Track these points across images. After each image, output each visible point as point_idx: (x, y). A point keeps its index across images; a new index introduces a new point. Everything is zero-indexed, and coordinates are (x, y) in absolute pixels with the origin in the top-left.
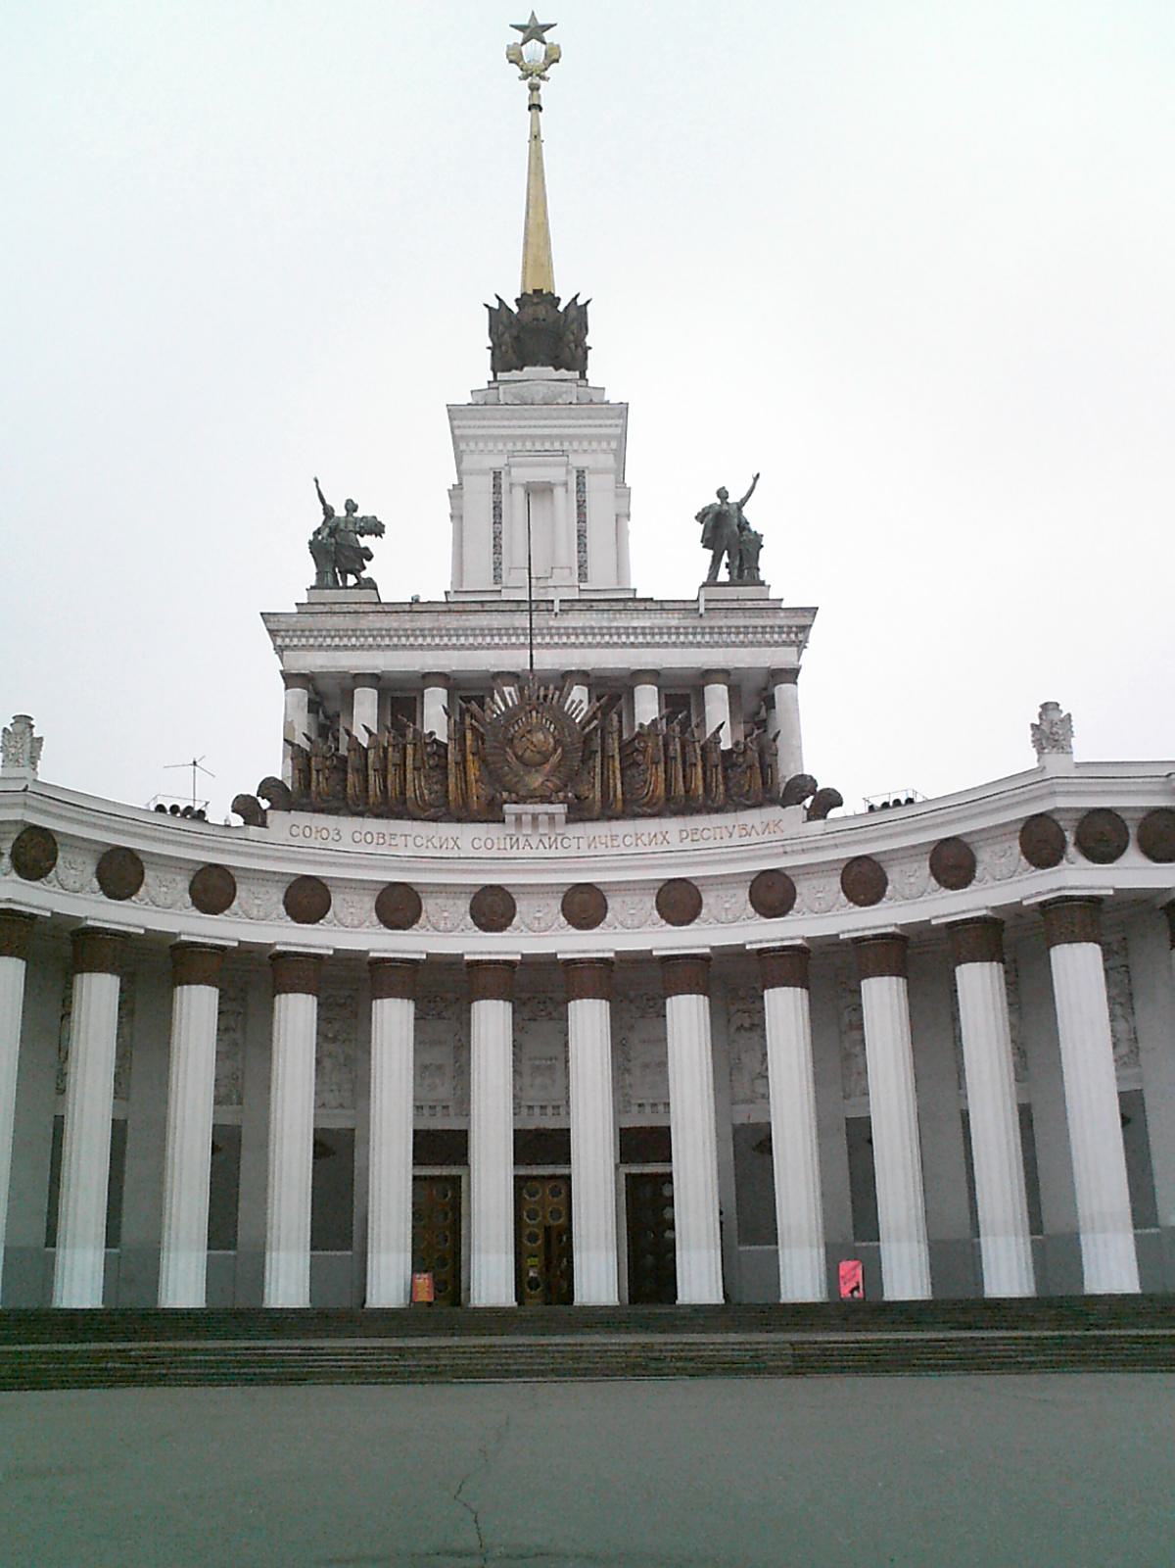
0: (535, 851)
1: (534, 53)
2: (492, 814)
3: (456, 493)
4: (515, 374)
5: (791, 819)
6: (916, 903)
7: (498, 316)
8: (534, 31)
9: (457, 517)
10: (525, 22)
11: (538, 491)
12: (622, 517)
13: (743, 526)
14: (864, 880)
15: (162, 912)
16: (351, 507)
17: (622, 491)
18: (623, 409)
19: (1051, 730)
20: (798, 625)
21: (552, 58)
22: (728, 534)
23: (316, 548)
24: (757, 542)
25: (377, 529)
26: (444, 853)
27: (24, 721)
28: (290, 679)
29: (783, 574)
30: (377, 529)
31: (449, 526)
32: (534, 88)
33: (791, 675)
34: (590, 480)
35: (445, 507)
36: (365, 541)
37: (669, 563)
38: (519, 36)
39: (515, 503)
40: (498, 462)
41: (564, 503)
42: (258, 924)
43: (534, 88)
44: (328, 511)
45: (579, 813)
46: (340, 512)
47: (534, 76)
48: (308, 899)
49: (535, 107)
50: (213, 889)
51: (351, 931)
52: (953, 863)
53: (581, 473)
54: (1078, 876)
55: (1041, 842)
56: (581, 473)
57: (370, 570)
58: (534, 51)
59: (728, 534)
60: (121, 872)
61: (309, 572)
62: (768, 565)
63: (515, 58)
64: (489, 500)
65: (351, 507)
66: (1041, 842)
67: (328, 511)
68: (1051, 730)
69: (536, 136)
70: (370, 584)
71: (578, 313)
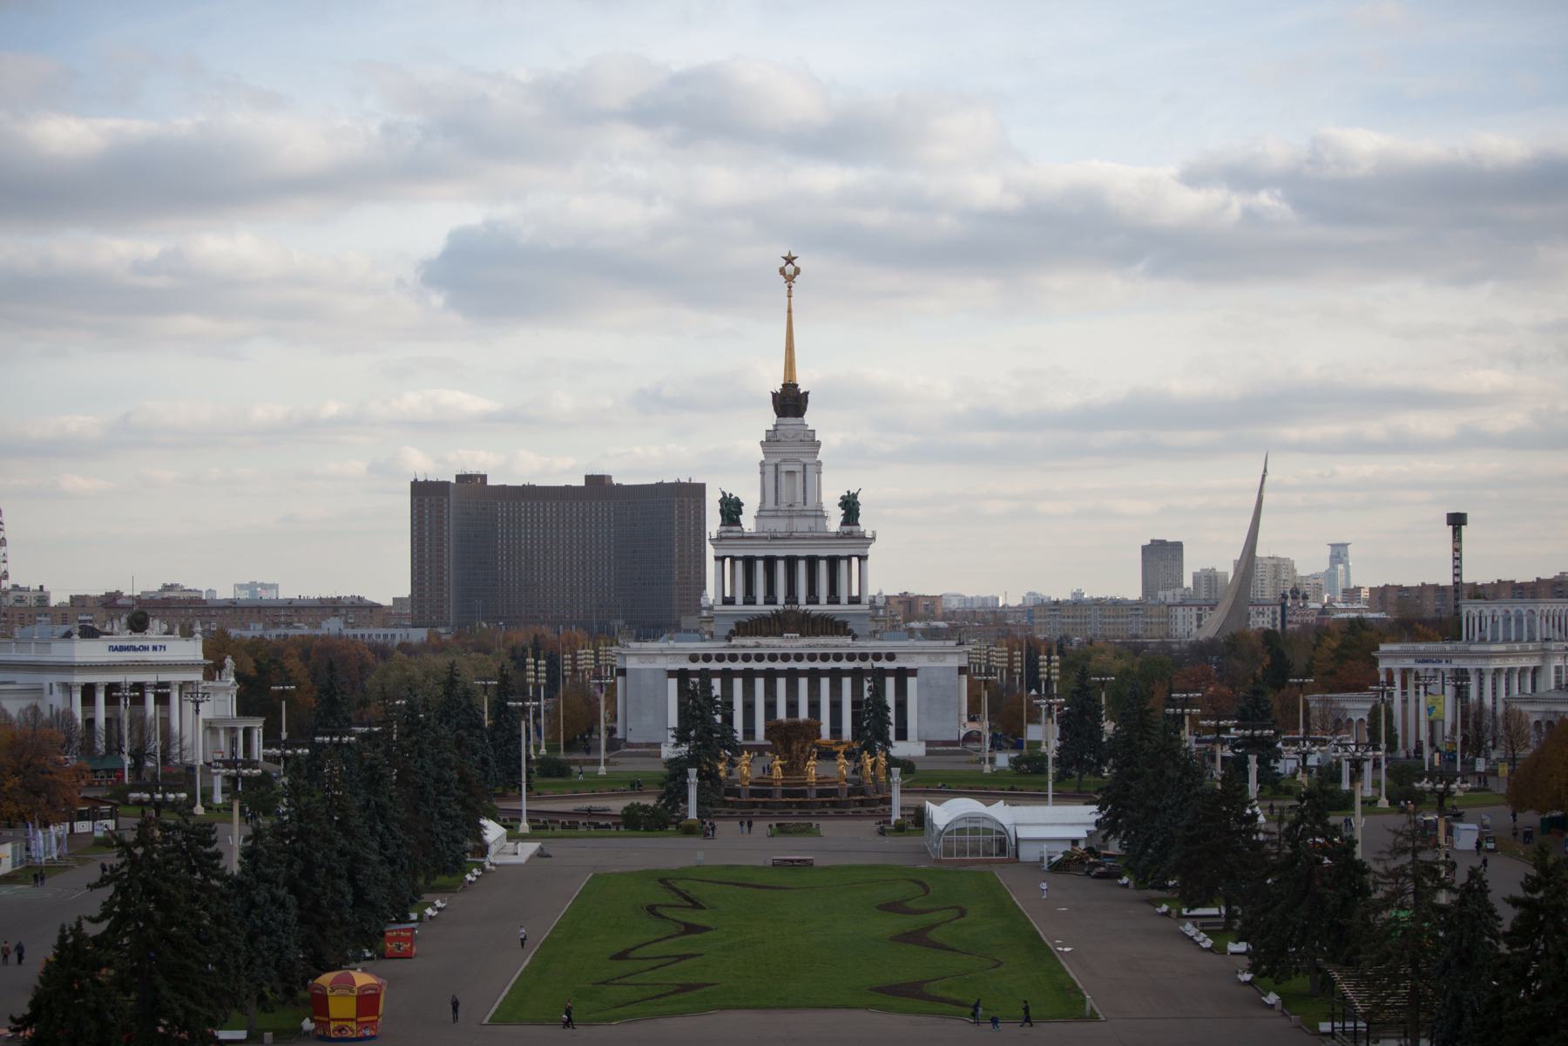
0: (792, 643)
3: (762, 464)
5: (849, 640)
7: (775, 395)
8: (790, 260)
9: (763, 473)
12: (819, 473)
17: (819, 463)
18: (818, 444)
22: (850, 506)
23: (722, 512)
29: (865, 524)
33: (865, 558)
35: (758, 469)
40: (777, 460)
41: (799, 477)
45: (803, 635)
58: (790, 269)
59: (850, 506)
69: (790, 311)
71: (806, 394)
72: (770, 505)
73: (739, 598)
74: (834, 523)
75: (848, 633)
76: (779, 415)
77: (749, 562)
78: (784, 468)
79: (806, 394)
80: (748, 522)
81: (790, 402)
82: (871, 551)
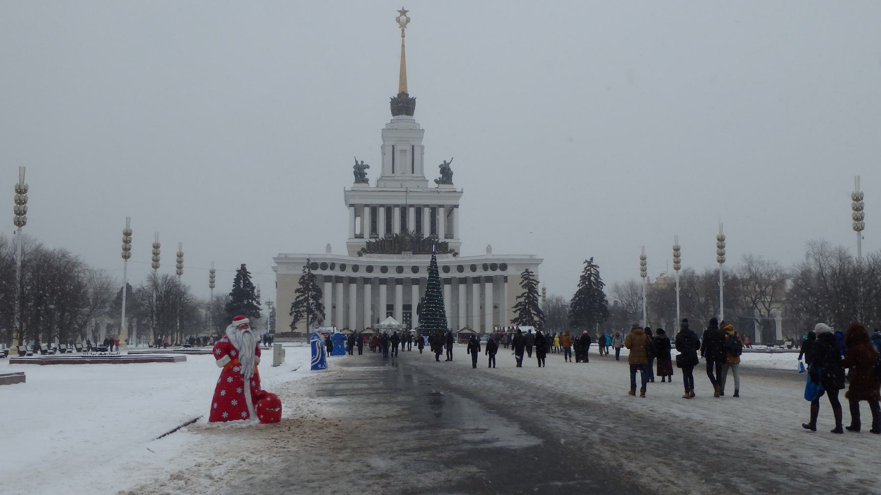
1: (403, 19)
2: (400, 253)
3: (383, 147)
4: (396, 117)
6: (467, 273)
8: (403, 12)
9: (384, 154)
10: (401, 9)
11: (403, 151)
12: (422, 154)
13: (449, 169)
14: (460, 269)
15: (349, 273)
16: (362, 162)
17: (422, 148)
19: (489, 249)
20: (458, 194)
21: (408, 20)
23: (355, 173)
24: (452, 174)
25: (368, 167)
26: (391, 260)
27: (329, 245)
28: (351, 205)
30: (368, 167)
31: (380, 157)
32: (403, 31)
34: (415, 149)
35: (380, 151)
36: (366, 171)
37: (432, 173)
38: (399, 14)
39: (397, 154)
40: (393, 143)
42: (362, 274)
43: (403, 31)
44: (357, 162)
46: (360, 163)
47: (403, 26)
48: (370, 269)
49: (403, 36)
50: (355, 268)
51: (377, 274)
52: (473, 268)
53: (413, 147)
54: (490, 273)
55: (485, 267)
56: (413, 147)
57: (367, 176)
60: (343, 267)
61: (353, 178)
62: (454, 179)
63: (398, 20)
64: (392, 154)
65: (362, 162)
66: (485, 267)
67: (357, 162)
68: (489, 249)
69: (403, 46)
70: (366, 181)
71: (413, 100)
72: (390, 173)
73: (367, 235)
74: (432, 185)
75: (451, 251)
76: (394, 114)
77: (374, 210)
78: (397, 148)
79: (413, 100)
80: (372, 184)
81: (403, 105)
82: (461, 202)
